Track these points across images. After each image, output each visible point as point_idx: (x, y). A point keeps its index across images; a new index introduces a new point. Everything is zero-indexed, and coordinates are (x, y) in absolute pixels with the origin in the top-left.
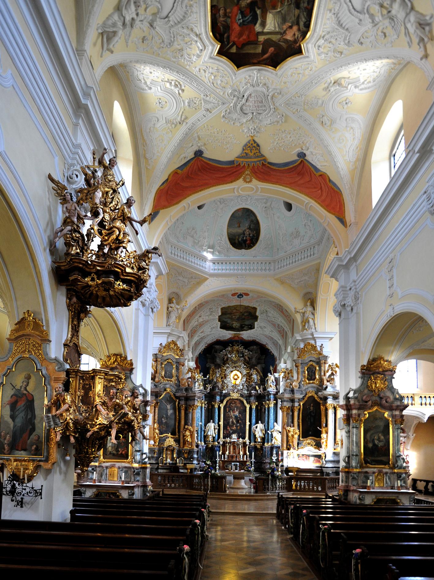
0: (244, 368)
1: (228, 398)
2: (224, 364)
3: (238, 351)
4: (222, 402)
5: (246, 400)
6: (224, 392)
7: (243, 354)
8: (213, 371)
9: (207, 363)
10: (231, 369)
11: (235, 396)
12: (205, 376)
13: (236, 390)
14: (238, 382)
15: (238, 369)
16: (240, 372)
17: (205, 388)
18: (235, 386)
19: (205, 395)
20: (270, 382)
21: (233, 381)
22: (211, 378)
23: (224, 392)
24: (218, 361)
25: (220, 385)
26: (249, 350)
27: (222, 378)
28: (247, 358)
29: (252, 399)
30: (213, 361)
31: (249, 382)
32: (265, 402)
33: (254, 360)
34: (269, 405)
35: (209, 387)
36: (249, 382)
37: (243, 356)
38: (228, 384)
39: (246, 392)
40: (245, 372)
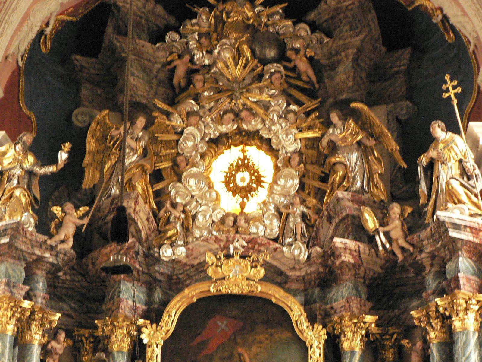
0: (284, 116)
1: (192, 293)
2: (173, 102)
3: (253, 32)
4: (154, 315)
5: (307, 305)
6: (166, 253)
7: (282, 48)
8: (103, 138)
9: (78, 104)
10: (213, 132)
11: (237, 277)
12: (44, 152)
13: (239, 244)
14: (252, 207)
15: (253, 125)
16: (267, 145)
17: (45, 224)
18: (233, 224)
19: (53, 272)
20: (448, 173)
21: (230, 204)
22: (90, 177)
23: (166, 253)
24: (136, 84)
25: (140, 213)
26: (314, 27)
27: (157, 176)
28: (303, 65)
29: (343, 294)
30: (110, 90)
31: (320, 194)
32: (425, 305)
33: (344, 73)
34: (445, 320)
35: (71, 219)
36: (320, 194)
37: (282, 58)
38: (192, 208)
39: (300, 251)
40: (291, 142)
